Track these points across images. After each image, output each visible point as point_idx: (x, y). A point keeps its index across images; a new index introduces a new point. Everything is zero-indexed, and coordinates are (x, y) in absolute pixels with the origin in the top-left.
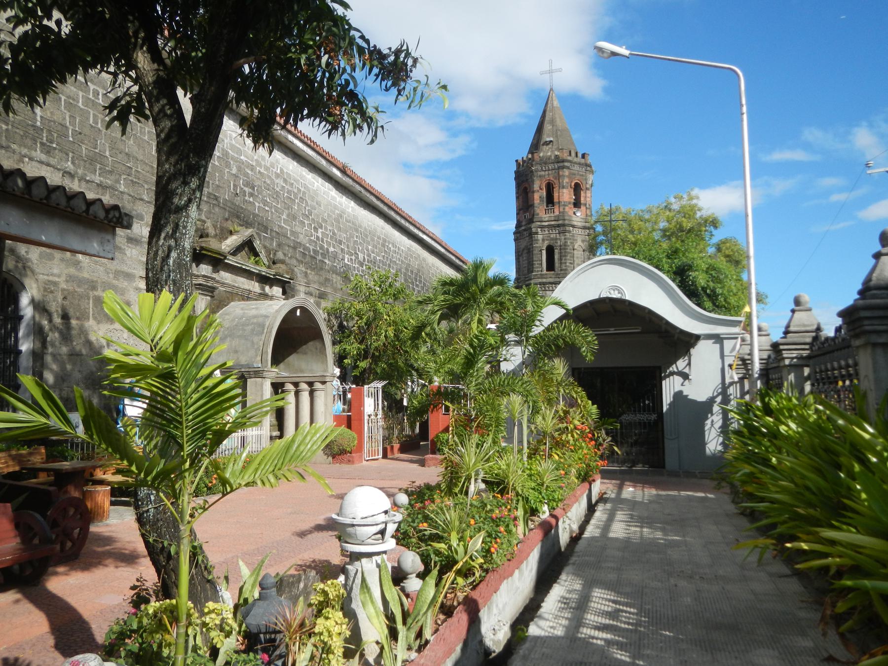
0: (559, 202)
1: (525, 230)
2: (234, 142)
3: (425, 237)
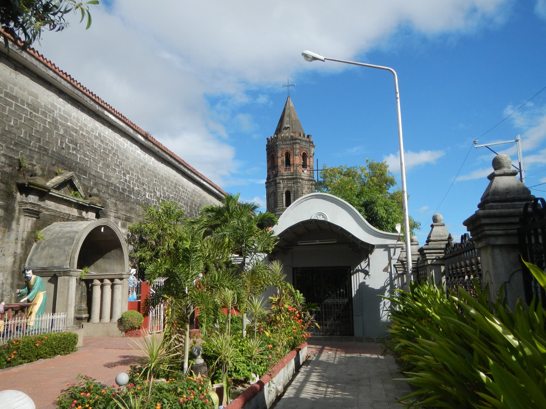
0: (293, 164)
1: (272, 181)
2: (62, 113)
3: (205, 183)
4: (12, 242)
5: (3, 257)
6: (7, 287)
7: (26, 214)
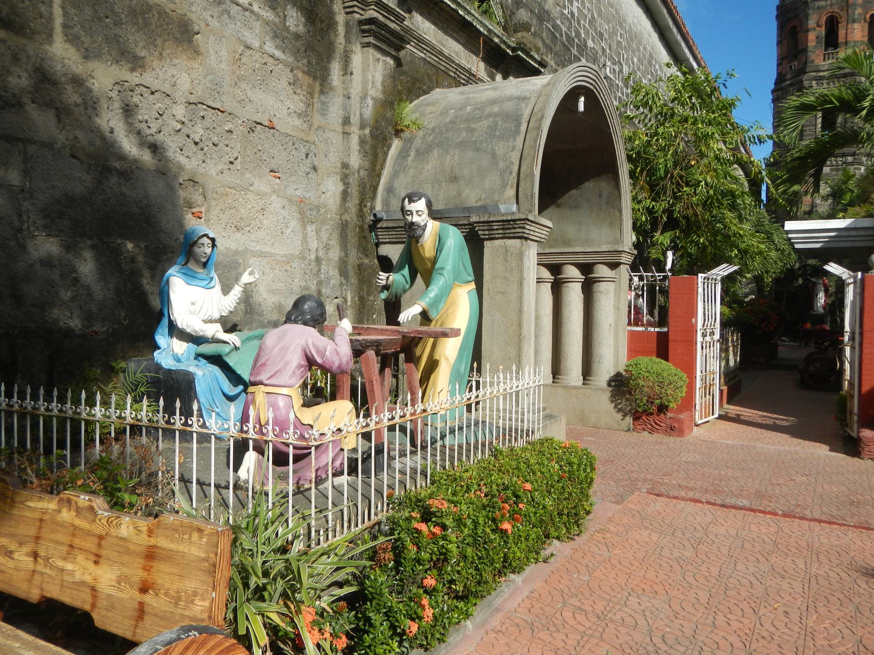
4: (335, 131)
5: (312, 175)
6: (331, 273)
7: (366, 40)
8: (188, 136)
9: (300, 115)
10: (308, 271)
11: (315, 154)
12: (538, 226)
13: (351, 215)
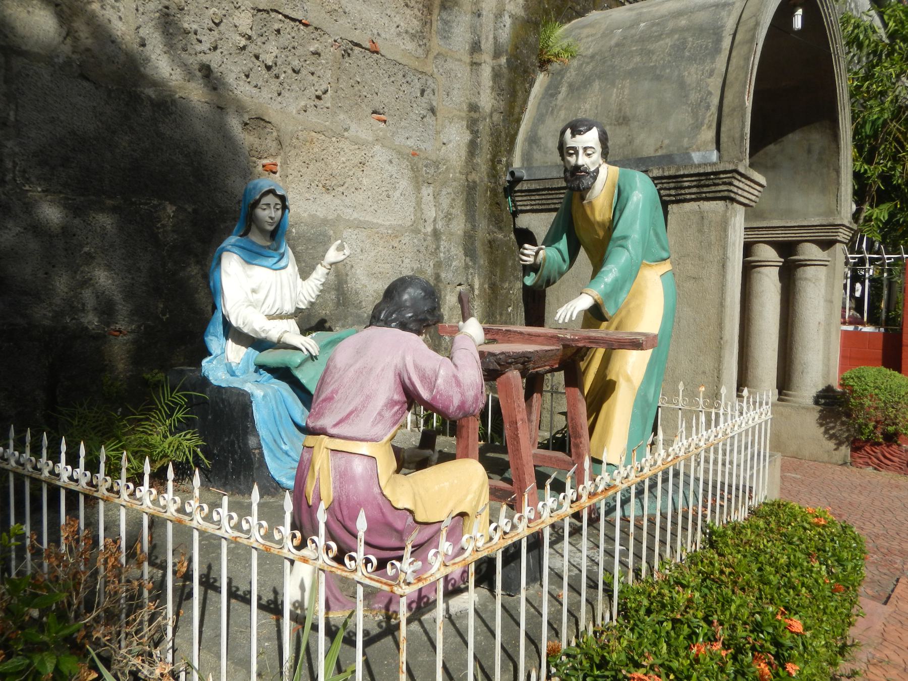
4: (460, 60)
5: (429, 119)
8: (257, 57)
9: (413, 37)
10: (423, 249)
11: (433, 90)
12: (749, 183)
13: (481, 175)
